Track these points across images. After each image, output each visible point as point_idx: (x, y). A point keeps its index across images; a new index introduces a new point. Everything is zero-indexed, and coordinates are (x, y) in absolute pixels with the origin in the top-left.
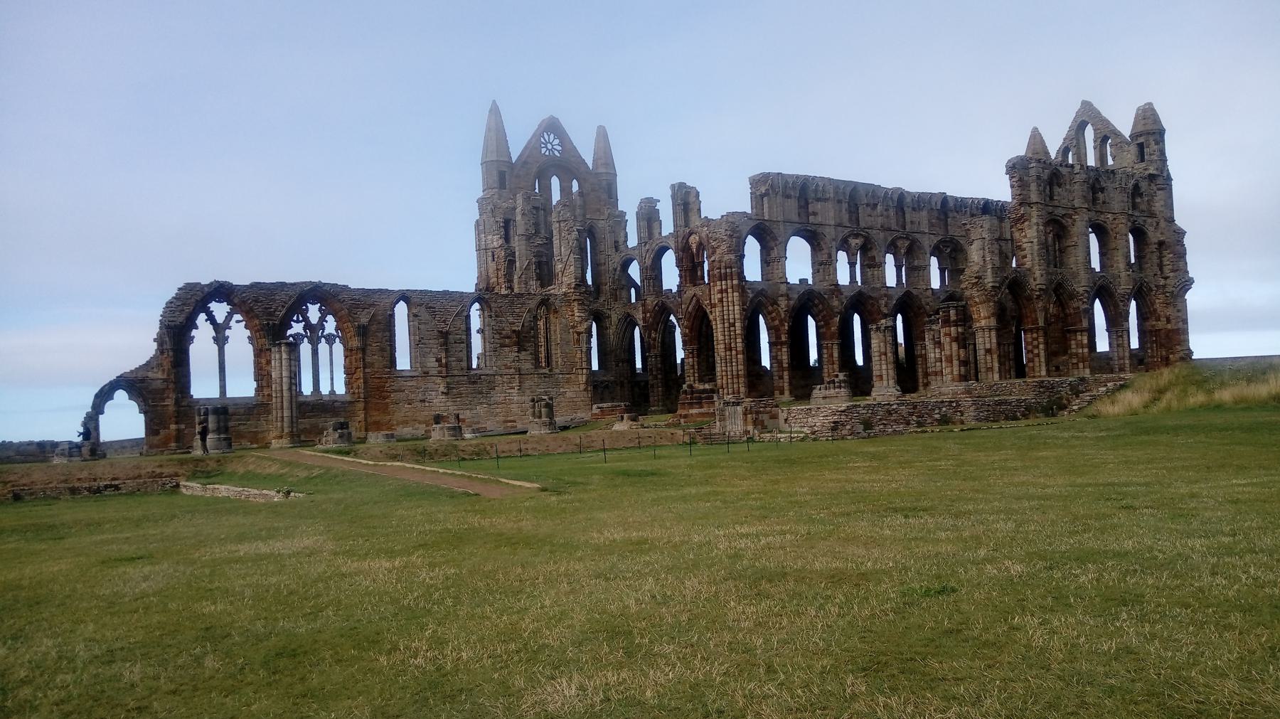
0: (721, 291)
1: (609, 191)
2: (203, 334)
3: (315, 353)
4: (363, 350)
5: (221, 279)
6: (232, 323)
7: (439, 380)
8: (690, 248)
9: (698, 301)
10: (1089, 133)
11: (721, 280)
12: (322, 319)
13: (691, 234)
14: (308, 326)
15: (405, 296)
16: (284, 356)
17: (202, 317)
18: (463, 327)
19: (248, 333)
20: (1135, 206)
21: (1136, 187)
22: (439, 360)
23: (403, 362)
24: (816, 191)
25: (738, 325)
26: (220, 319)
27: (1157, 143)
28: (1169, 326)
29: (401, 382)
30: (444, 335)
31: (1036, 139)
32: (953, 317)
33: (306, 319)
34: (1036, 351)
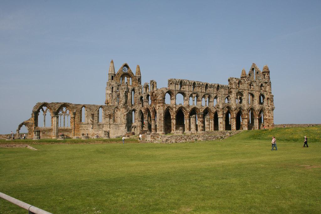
0: (159, 106)
1: (139, 80)
4: (74, 118)
7: (91, 125)
9: (154, 108)
13: (154, 92)
16: (56, 119)
17: (41, 110)
18: (97, 113)
20: (261, 89)
21: (262, 85)
22: (91, 120)
24: (184, 83)
25: (162, 114)
26: (45, 110)
27: (268, 75)
28: (269, 118)
30: (93, 115)
32: (200, 116)
34: (233, 123)
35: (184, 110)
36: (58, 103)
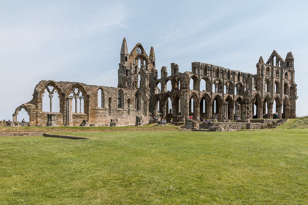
0: (184, 92)
2: (46, 94)
3: (76, 101)
5: (52, 80)
6: (54, 92)
8: (175, 80)
10: (275, 58)
11: (184, 89)
12: (79, 92)
13: (176, 76)
14: (74, 94)
15: (101, 88)
19: (58, 95)
23: (100, 105)
26: (51, 91)
29: (99, 111)
31: (261, 60)
33: (74, 92)
35: (208, 98)
36: (68, 82)
